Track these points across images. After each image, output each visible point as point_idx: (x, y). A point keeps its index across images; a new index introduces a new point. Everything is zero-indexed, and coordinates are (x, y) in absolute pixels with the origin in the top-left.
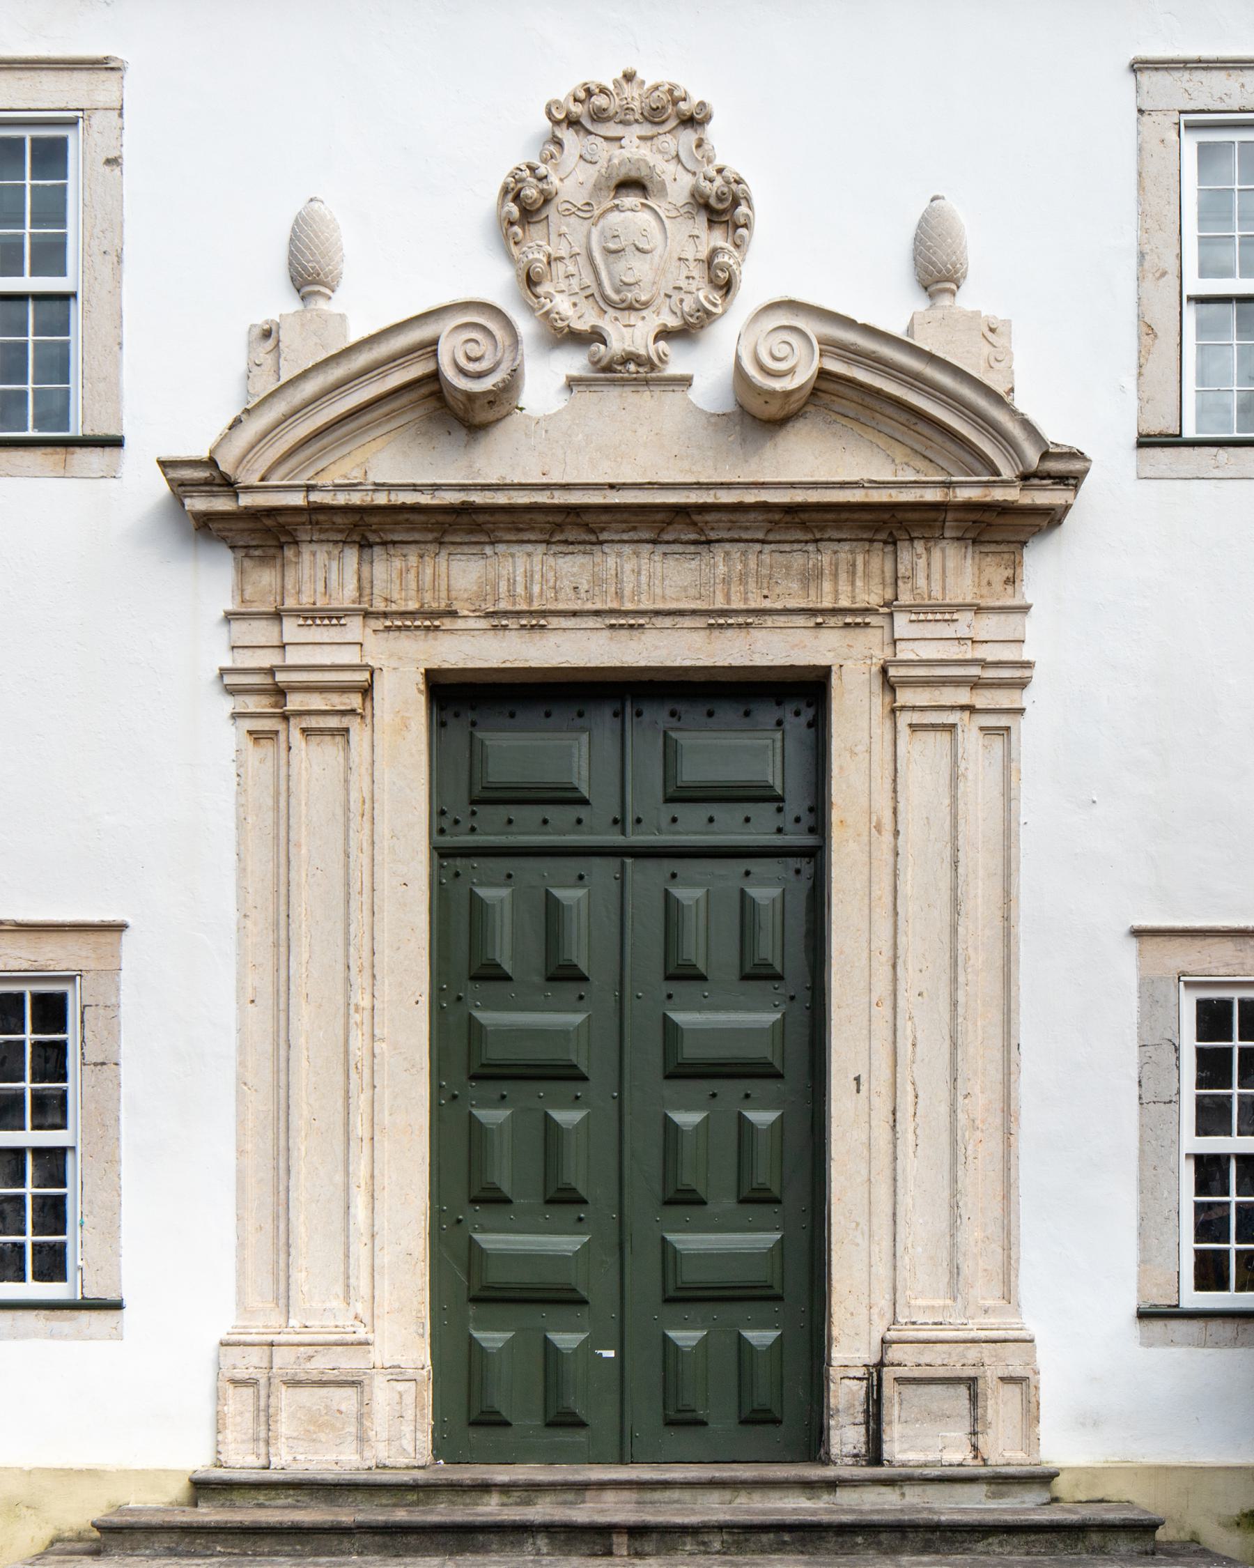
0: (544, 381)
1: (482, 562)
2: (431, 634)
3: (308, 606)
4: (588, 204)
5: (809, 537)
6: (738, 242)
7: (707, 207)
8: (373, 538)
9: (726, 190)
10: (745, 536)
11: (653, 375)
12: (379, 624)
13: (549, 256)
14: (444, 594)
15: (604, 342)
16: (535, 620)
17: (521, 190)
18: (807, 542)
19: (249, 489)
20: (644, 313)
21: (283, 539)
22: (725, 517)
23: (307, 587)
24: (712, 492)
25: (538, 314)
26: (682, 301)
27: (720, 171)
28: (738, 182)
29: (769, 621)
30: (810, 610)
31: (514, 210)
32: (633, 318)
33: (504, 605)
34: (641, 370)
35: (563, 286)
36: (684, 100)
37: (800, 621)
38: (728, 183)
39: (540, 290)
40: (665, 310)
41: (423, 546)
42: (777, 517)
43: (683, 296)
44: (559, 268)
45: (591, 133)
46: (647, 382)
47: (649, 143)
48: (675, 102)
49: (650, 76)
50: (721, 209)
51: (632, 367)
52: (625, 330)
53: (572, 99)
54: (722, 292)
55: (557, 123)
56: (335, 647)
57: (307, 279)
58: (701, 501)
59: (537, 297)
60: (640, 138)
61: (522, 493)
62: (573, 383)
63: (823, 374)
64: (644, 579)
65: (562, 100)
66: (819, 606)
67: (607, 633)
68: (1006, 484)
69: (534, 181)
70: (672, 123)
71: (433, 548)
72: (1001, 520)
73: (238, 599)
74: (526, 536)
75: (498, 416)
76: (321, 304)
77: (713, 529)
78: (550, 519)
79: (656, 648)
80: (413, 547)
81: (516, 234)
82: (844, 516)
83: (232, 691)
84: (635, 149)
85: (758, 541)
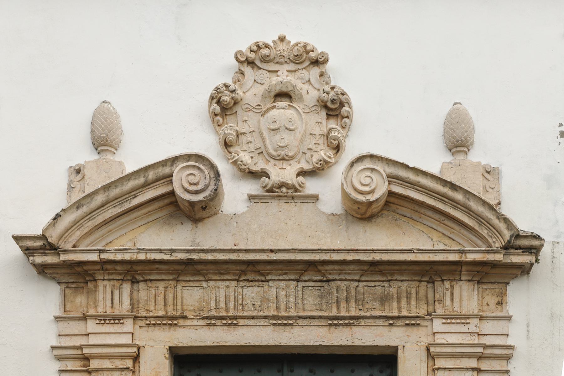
0: (235, 195)
1: (201, 291)
2: (172, 328)
3: (102, 313)
4: (259, 105)
5: (385, 278)
6: (344, 126)
7: (326, 107)
8: (139, 278)
9: (336, 98)
10: (348, 278)
11: (296, 194)
12: (142, 323)
13: (237, 132)
14: (179, 307)
15: (269, 178)
16: (231, 322)
17: (220, 97)
18: (383, 281)
19: (66, 251)
20: (291, 162)
21: (88, 279)
22: (336, 267)
23: (100, 304)
24: (328, 254)
25: (231, 161)
26: (312, 156)
27: (333, 88)
28: (343, 94)
29: (363, 322)
30: (386, 317)
31: (218, 109)
32: (285, 164)
33: (213, 313)
34: (289, 191)
35: (245, 148)
36: (313, 51)
37: (380, 322)
38: (337, 94)
39: (231, 150)
40: (303, 161)
41: (167, 282)
42: (366, 268)
43: (313, 153)
44: (243, 139)
45: (261, 69)
46: (293, 198)
47: (293, 74)
48: (308, 52)
49: (293, 39)
50: (335, 108)
51: (284, 190)
52: (279, 170)
54: (335, 151)
55: (241, 62)
56: (117, 335)
57: (103, 141)
58: (322, 259)
59: (230, 153)
60: (288, 71)
61: (221, 254)
62: (251, 197)
63: (391, 194)
64: (292, 299)
65: (244, 51)
66: (391, 315)
67: (272, 328)
68: (495, 252)
69: (228, 93)
70: (307, 63)
71: (173, 283)
72: (493, 271)
73: (63, 310)
74: (225, 277)
75: (209, 214)
76: (110, 157)
77: (330, 274)
78: (238, 268)
79: (299, 336)
80: (162, 283)
81: (219, 120)
82: (404, 267)
83: (60, 358)
84: (284, 77)
85: (356, 281)
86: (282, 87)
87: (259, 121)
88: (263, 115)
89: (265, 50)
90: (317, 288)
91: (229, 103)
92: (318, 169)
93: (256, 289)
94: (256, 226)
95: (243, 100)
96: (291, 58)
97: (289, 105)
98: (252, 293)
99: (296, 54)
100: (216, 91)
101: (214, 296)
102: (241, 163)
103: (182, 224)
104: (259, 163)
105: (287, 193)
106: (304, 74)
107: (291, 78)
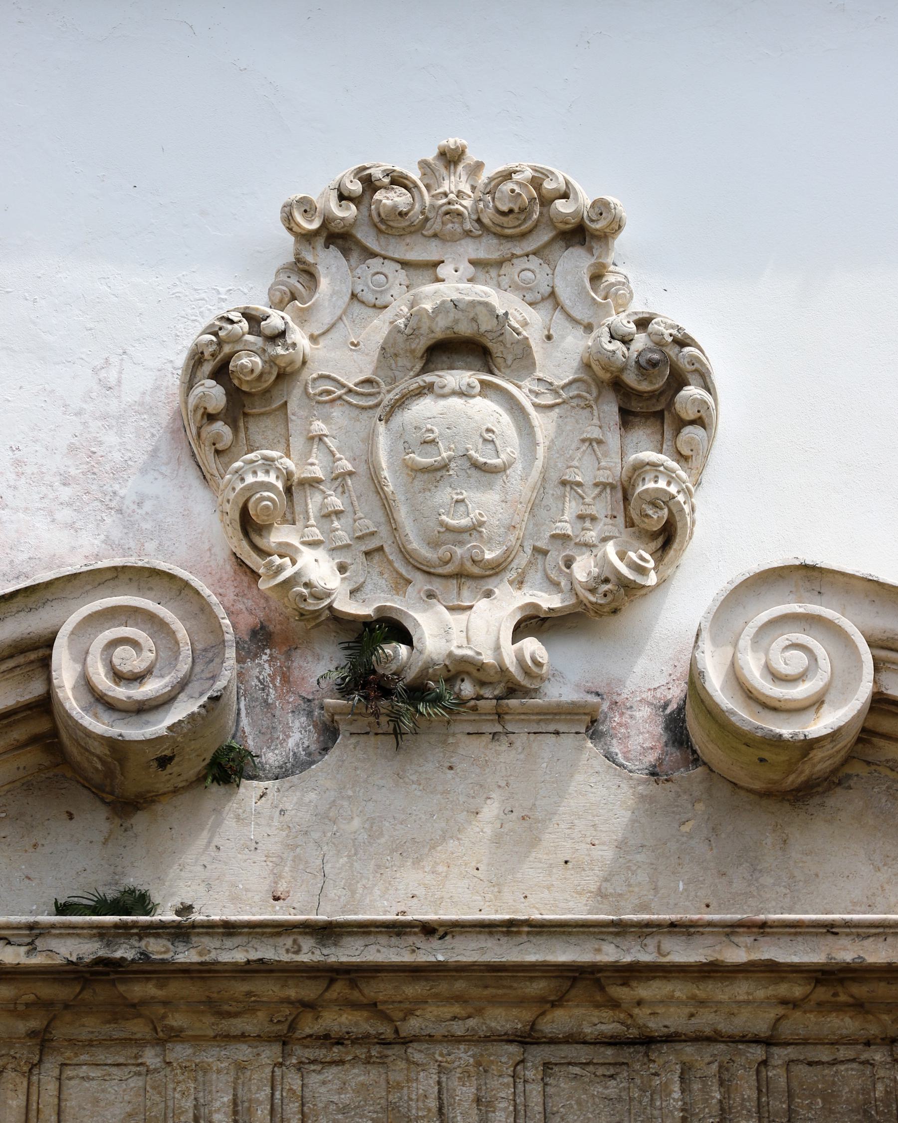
6: (686, 451)
7: (617, 385)
13: (289, 476)
20: (490, 584)
26: (569, 563)
27: (643, 323)
34: (487, 692)
35: (316, 533)
36: (565, 196)
45: (374, 255)
47: (493, 273)
50: (651, 392)
53: (334, 194)
78: (292, 993)
81: (219, 436)
86: (456, 321)
87: (371, 439)
88: (387, 418)
89: (391, 194)
90: (601, 1071)
91: (261, 375)
92: (598, 610)
93: (357, 1075)
94: (356, 823)
95: (310, 365)
96: (486, 221)
97: (482, 382)
98: (341, 1090)
99: (505, 209)
100: (215, 334)
101: (189, 1104)
102: (305, 591)
103: (71, 816)
104: (369, 587)
105: (479, 698)
106: (534, 272)
107: (485, 292)
